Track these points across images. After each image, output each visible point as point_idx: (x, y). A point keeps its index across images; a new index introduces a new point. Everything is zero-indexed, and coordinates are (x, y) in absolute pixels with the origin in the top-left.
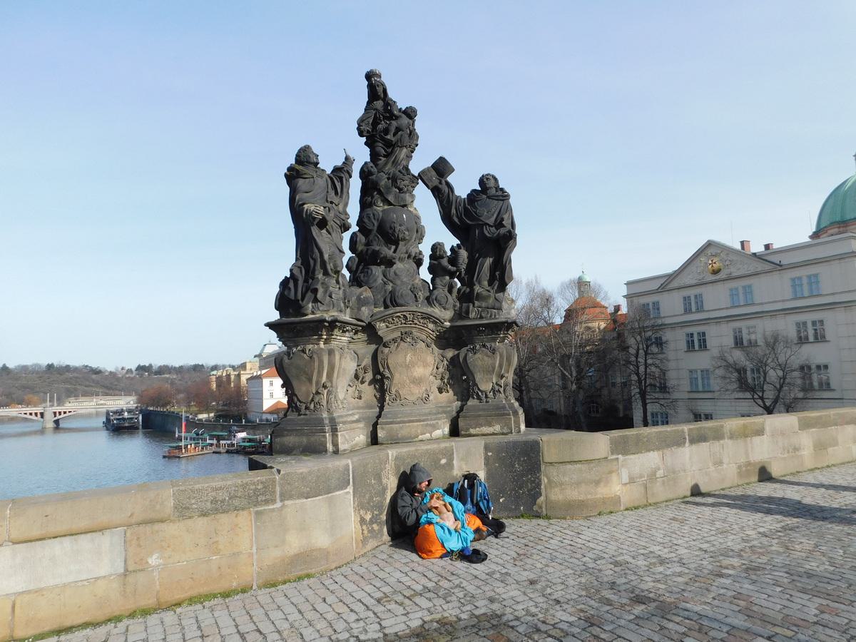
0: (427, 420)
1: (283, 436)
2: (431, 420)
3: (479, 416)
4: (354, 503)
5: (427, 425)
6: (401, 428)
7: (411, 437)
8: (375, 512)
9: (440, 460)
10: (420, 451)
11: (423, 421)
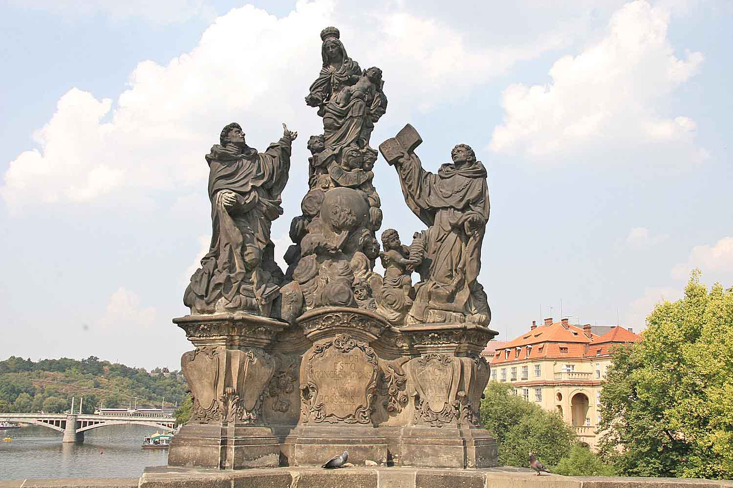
0: (358, 442)
1: (179, 446)
2: (364, 442)
3: (426, 443)
11: (353, 443)
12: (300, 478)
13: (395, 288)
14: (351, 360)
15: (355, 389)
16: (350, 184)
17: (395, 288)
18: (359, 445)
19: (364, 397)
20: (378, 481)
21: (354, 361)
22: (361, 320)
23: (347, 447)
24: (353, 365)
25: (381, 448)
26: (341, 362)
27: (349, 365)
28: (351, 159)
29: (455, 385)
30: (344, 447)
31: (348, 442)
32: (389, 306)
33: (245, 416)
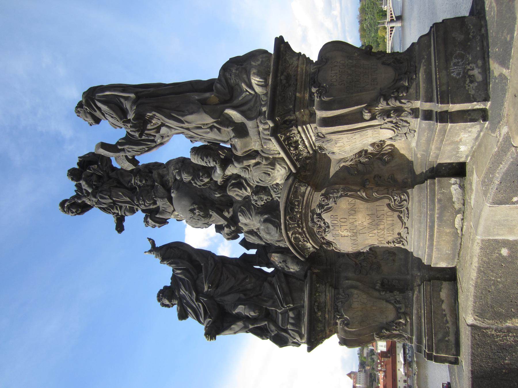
0: (432, 216)
2: (433, 210)
5: (440, 219)
9: (500, 254)
10: (479, 281)
11: (433, 222)
12: (477, 316)
13: (251, 171)
14: (335, 222)
16: (169, 203)
17: (251, 171)
19: (377, 203)
20: (491, 238)
22: (292, 210)
23: (438, 229)
24: (342, 220)
26: (340, 231)
27: (343, 224)
28: (148, 204)
29: (356, 126)
30: (437, 232)
31: (432, 228)
32: (271, 175)
33: (402, 321)
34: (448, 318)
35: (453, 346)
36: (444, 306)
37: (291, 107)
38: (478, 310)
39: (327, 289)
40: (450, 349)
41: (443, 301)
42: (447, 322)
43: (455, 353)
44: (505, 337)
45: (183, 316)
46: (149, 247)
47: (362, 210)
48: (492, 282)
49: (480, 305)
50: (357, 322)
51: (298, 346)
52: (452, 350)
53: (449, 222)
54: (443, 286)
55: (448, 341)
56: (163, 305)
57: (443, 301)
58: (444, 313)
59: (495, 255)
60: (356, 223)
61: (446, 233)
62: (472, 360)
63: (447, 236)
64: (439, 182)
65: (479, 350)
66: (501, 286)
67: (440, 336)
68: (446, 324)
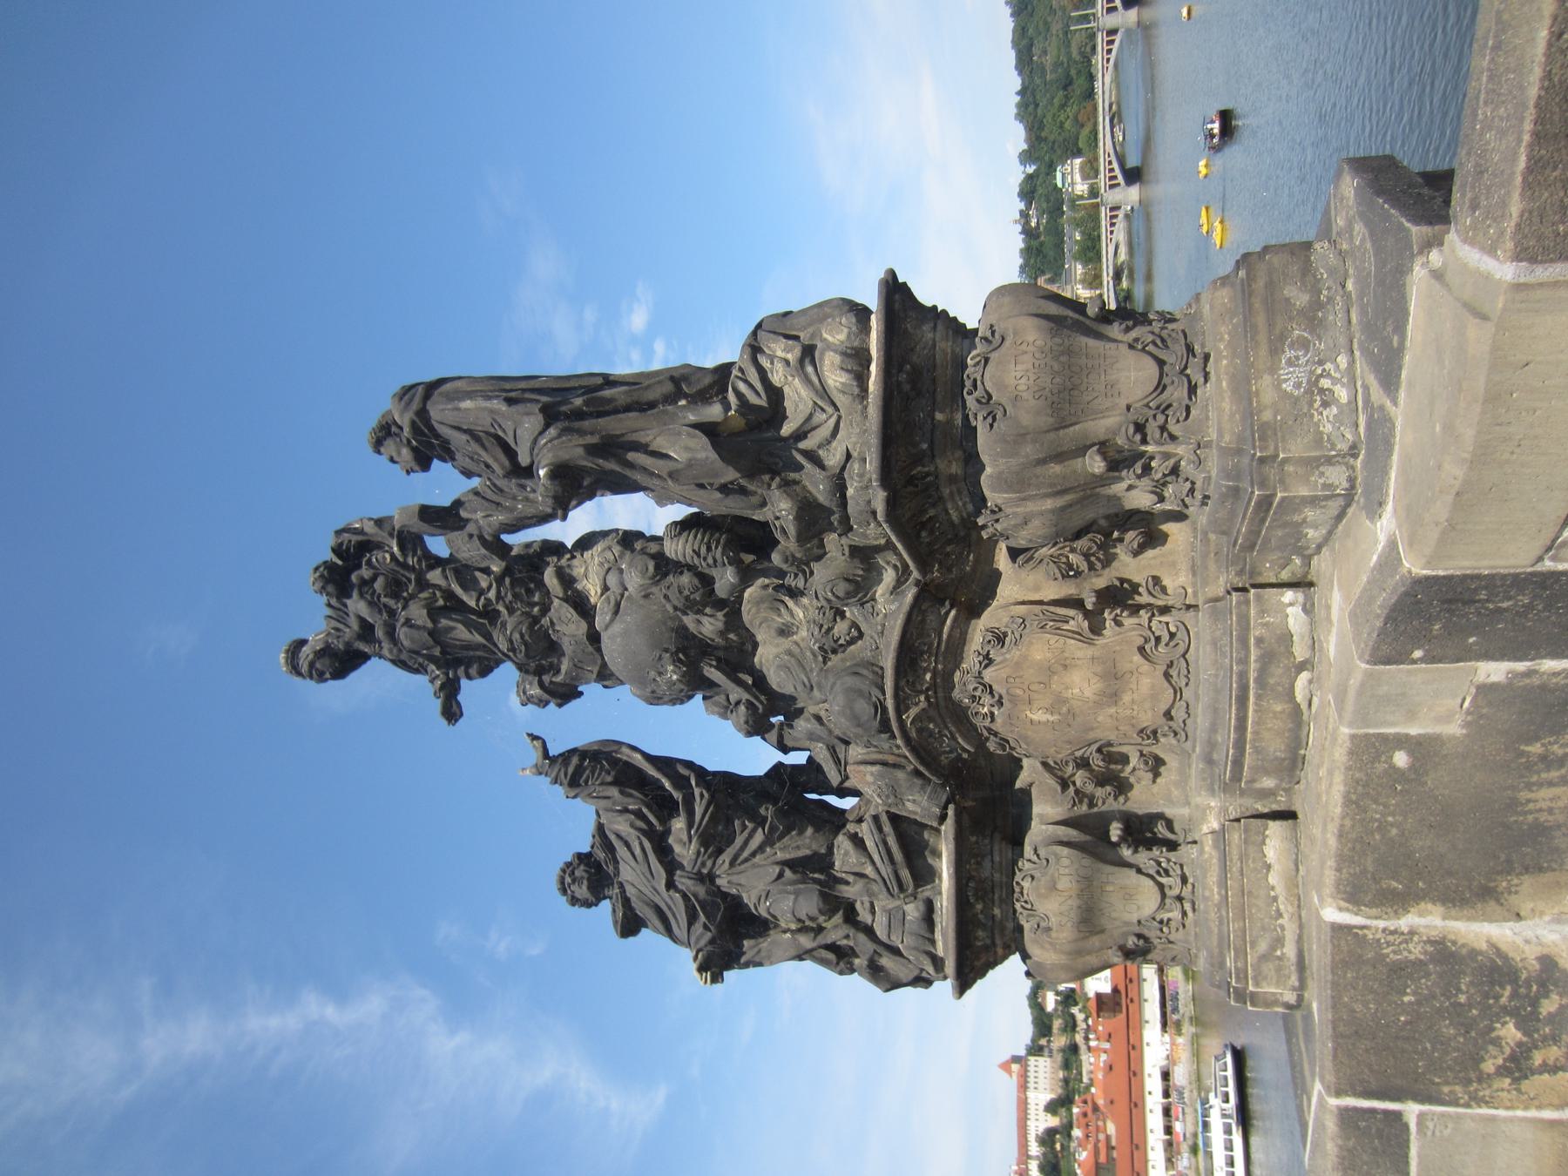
0: (1243, 675)
2: (1244, 661)
4: (1455, 1103)
5: (1261, 681)
6: (1257, 750)
7: (1290, 730)
8: (1503, 1000)
9: (1393, 767)
10: (1348, 822)
11: (1244, 689)
14: (1019, 692)
15: (1095, 674)
18: (1252, 676)
20: (1371, 731)
21: (1021, 686)
23: (1256, 704)
25: (1262, 612)
26: (1028, 713)
30: (1255, 711)
34: (1282, 907)
35: (1293, 968)
36: (1273, 879)
37: (925, 446)
38: (1345, 886)
39: (996, 847)
40: (1285, 975)
41: (1269, 867)
42: (1280, 915)
43: (1297, 984)
44: (1405, 945)
45: (630, 925)
46: (533, 755)
47: (1079, 662)
48: (1376, 824)
49: (1350, 873)
50: (1069, 924)
51: (927, 988)
52: (1289, 978)
53: (1280, 689)
54: (1267, 833)
55: (1280, 958)
56: (574, 901)
57: (1269, 867)
58: (1272, 893)
59: (1380, 767)
60: (1068, 694)
61: (1275, 713)
62: (1333, 997)
63: (1277, 719)
64: (1258, 598)
65: (1349, 975)
66: (1394, 831)
67: (1263, 946)
68: (1277, 919)
